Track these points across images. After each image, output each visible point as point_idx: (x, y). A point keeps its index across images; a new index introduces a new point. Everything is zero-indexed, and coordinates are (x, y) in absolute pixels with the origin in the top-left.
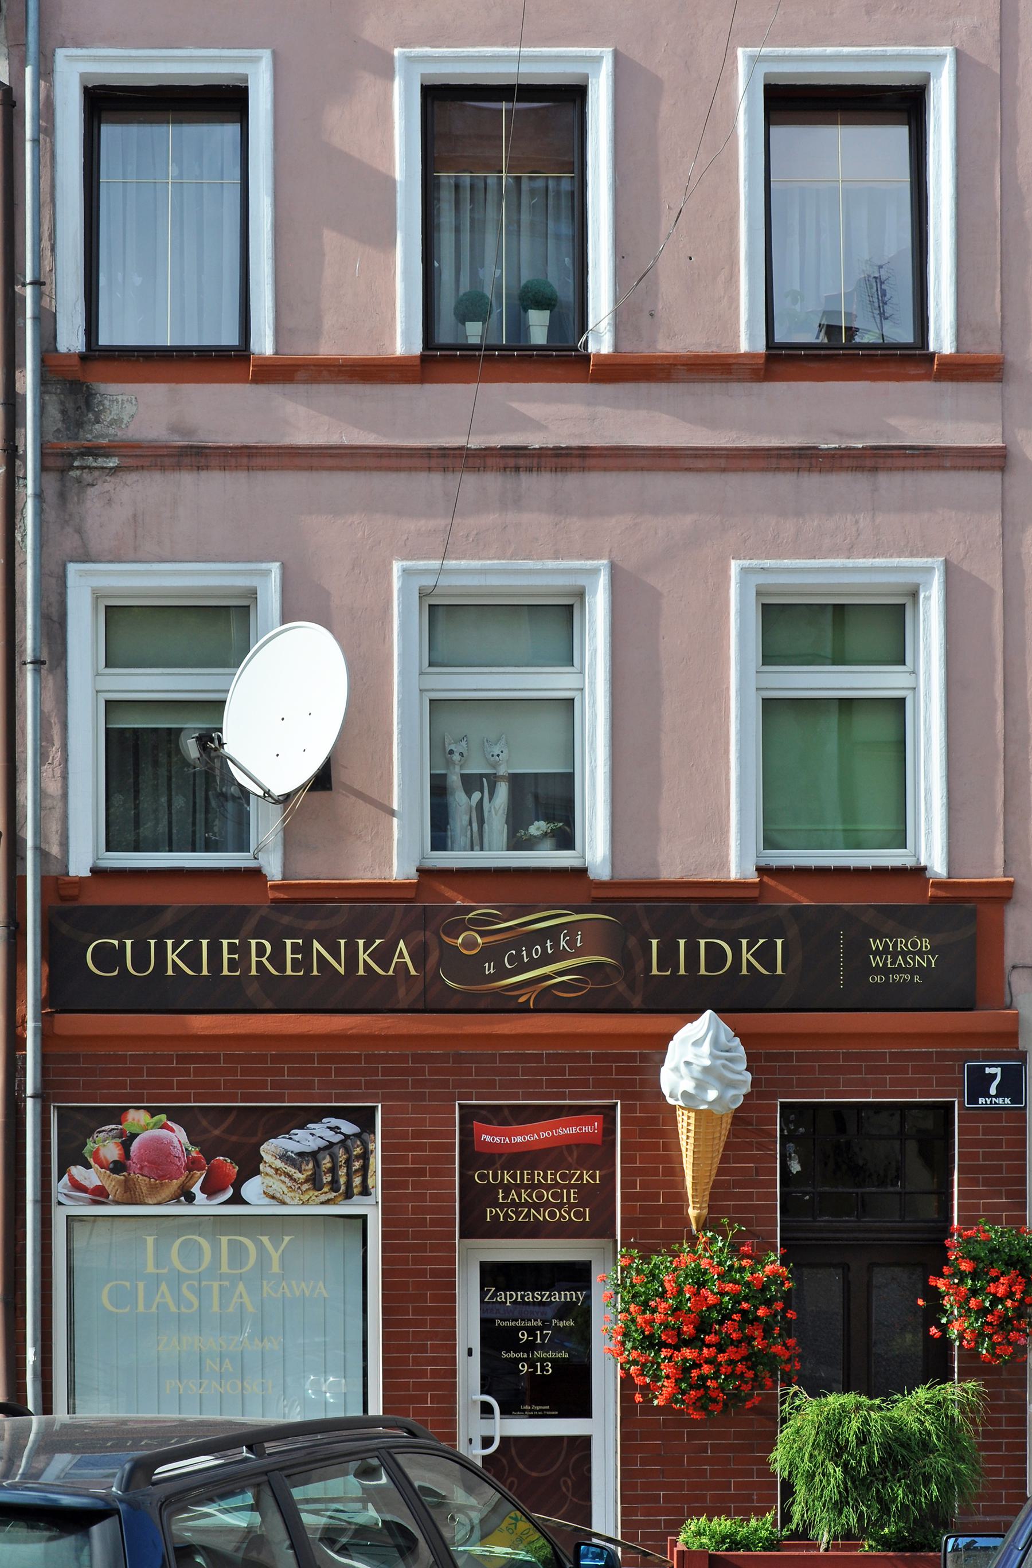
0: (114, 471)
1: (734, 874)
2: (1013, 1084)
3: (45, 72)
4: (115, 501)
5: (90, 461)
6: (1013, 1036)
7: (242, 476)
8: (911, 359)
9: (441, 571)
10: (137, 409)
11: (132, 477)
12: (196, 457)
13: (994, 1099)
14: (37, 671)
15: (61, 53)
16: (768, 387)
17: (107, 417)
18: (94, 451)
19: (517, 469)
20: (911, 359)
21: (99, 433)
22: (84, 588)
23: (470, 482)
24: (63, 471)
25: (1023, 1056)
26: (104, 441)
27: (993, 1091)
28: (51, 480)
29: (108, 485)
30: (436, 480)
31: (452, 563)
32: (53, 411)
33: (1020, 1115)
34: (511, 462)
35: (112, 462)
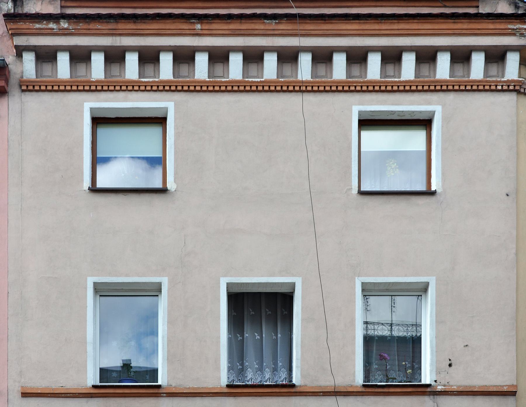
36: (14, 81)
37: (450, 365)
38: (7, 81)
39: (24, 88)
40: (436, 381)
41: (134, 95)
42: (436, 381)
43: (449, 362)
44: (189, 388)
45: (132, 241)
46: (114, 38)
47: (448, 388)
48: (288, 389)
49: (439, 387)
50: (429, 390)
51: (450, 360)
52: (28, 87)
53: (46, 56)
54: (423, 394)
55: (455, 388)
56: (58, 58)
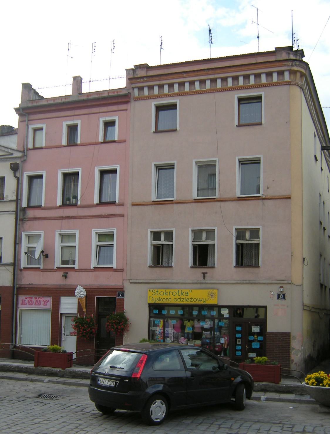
0: (27, 221)
1: (92, 268)
2: (123, 295)
3: (22, 175)
4: (28, 224)
5: (25, 220)
6: (123, 289)
7: (40, 221)
8: (113, 203)
9: (60, 232)
10: (31, 213)
11: (29, 222)
12: (35, 219)
13: (120, 297)
14: (18, 245)
15: (24, 173)
16: (97, 208)
17: (27, 215)
18: (25, 218)
19: (69, 219)
20: (113, 203)
21: (27, 216)
22: (23, 234)
23: (64, 221)
24: (22, 221)
25: (124, 291)
26: (27, 217)
27: (120, 296)
28: (21, 222)
29: (27, 222)
30: (60, 221)
31: (61, 231)
32: (22, 214)
33: (123, 299)
34: (68, 218)
35: (27, 220)
36: (132, 97)
37: (268, 188)
38: (130, 98)
39: (135, 100)
40: (263, 194)
41: (167, 98)
42: (263, 194)
43: (267, 187)
44: (182, 201)
45: (165, 149)
46: (160, 81)
47: (267, 197)
48: (214, 200)
49: (264, 197)
50: (260, 198)
51: (268, 186)
52: (137, 99)
53: (141, 89)
54: (259, 199)
55: (269, 197)
56: (144, 89)
